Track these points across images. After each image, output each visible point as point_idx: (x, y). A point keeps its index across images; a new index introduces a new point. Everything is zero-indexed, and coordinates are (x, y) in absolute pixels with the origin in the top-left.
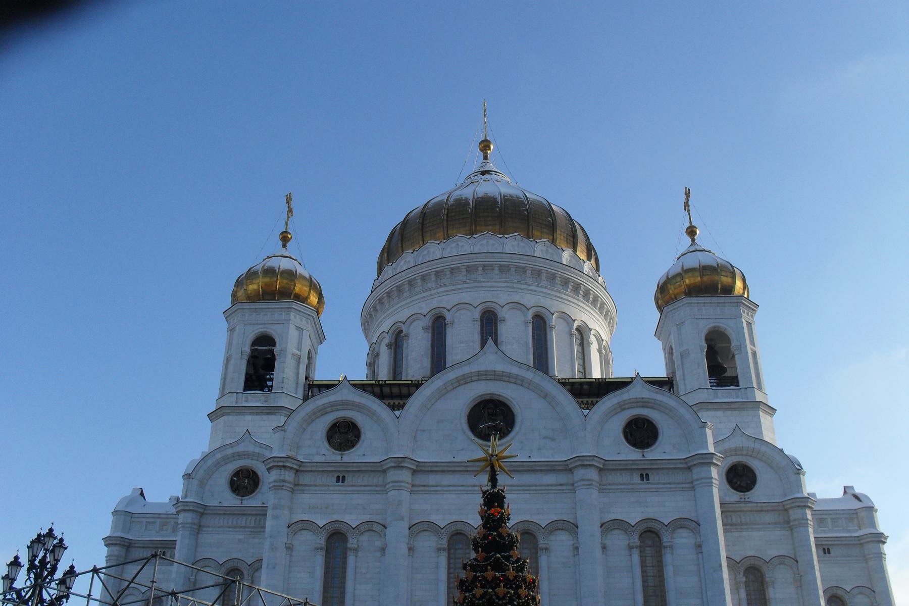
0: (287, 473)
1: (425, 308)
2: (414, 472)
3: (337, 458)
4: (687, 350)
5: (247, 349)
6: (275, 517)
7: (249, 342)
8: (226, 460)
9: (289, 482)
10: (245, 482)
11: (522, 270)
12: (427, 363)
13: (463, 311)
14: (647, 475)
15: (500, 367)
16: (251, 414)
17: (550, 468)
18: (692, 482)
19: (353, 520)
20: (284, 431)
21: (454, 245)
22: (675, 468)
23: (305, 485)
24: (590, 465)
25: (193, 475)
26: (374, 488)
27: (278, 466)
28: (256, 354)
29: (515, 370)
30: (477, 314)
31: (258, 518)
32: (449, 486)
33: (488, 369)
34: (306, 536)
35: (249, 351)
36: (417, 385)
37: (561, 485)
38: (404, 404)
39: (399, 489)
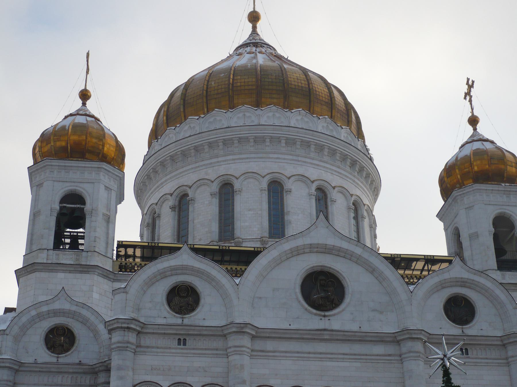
0: (130, 334)
1: (212, 174)
2: (254, 337)
3: (179, 321)
4: (476, 232)
5: (57, 207)
6: (121, 378)
7: (58, 199)
9: (132, 344)
10: (60, 339)
11: (306, 144)
12: (215, 227)
13: (251, 180)
14: (466, 349)
15: (332, 241)
16: (64, 271)
17: (380, 339)
18: (507, 359)
20: (126, 293)
21: (241, 115)
22: (491, 345)
23: (148, 347)
24: (417, 338)
25: (7, 332)
26: (215, 352)
27: (121, 328)
28: (65, 211)
29: (345, 245)
30: (265, 184)
31: (75, 376)
32: (286, 352)
33: (320, 242)
35: (58, 208)
36: (254, 254)
37: (390, 355)
38: (243, 272)
39: (241, 354)
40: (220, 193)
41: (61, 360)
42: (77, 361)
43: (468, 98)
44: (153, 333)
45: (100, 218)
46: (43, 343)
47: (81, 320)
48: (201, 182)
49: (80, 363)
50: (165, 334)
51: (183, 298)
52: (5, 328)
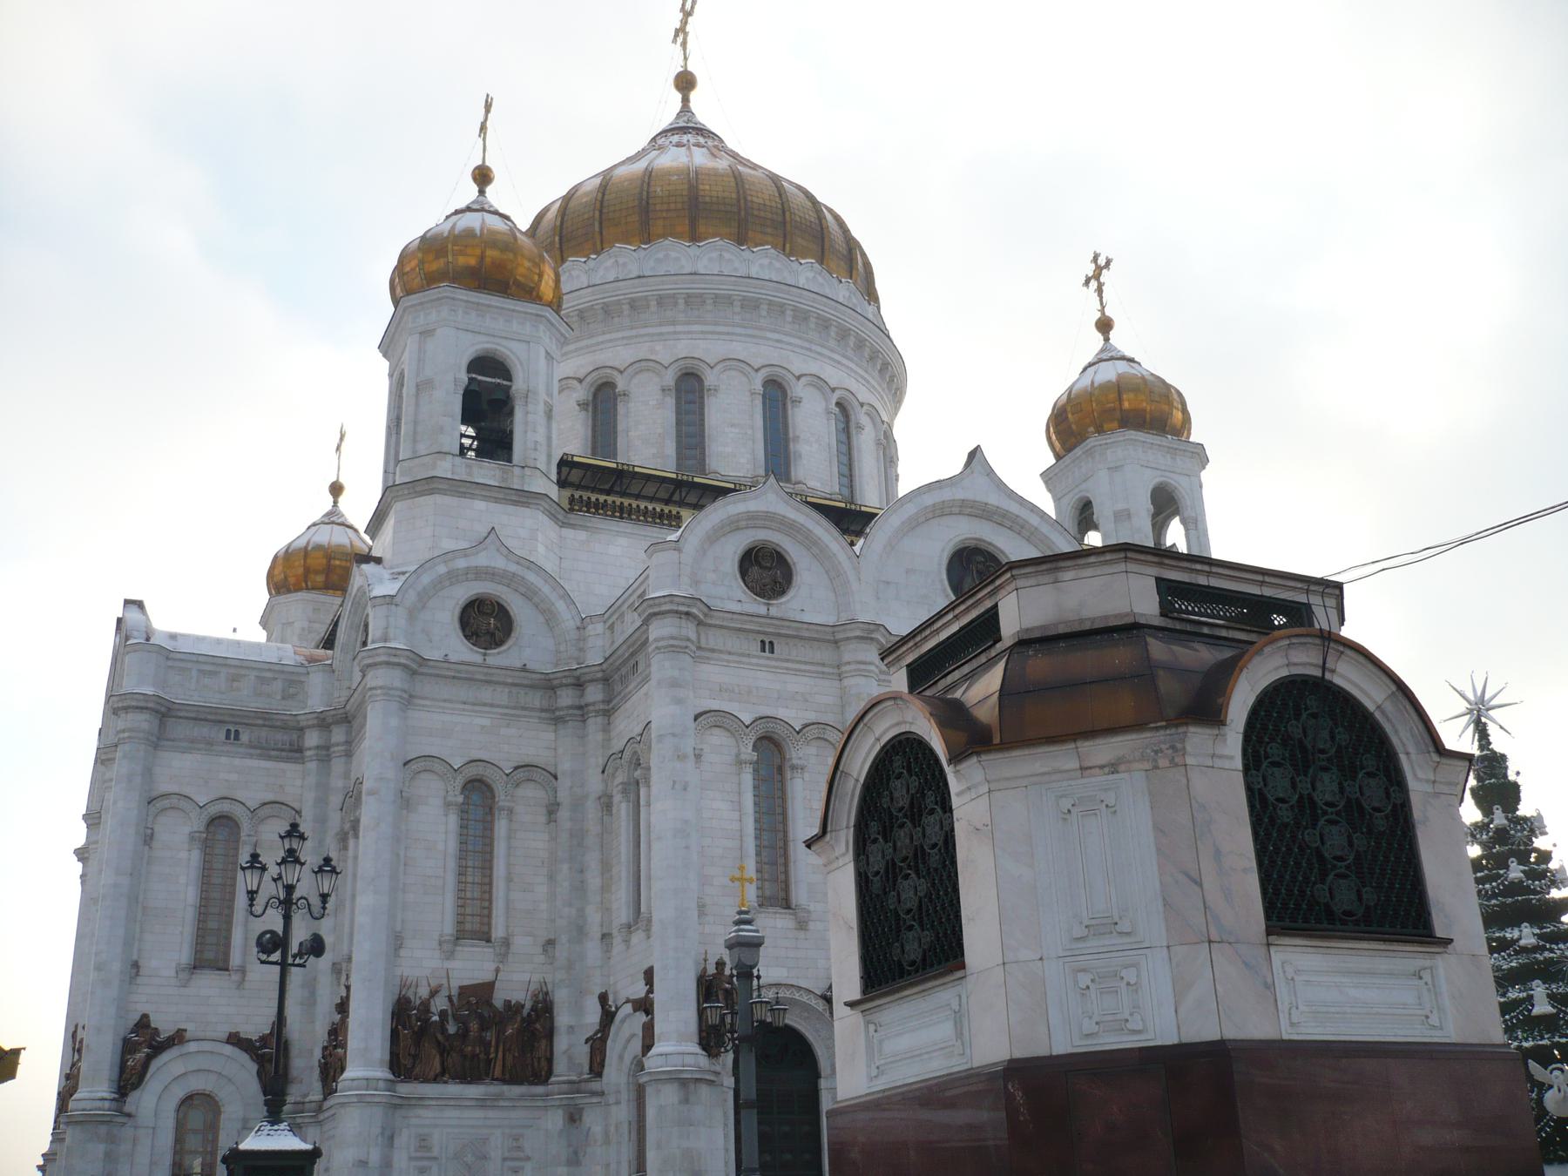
3: (762, 610)
4: (1128, 510)
8: (453, 577)
13: (733, 373)
16: (485, 498)
19: (794, 716)
20: (679, 550)
23: (713, 651)
25: (397, 600)
26: (820, 669)
27: (677, 612)
28: (474, 387)
31: (514, 690)
34: (718, 738)
40: (678, 390)
41: (491, 660)
42: (519, 665)
43: (1094, 284)
44: (721, 627)
45: (541, 408)
46: (457, 625)
47: (523, 590)
48: (643, 365)
49: (524, 669)
50: (739, 630)
51: (766, 570)
52: (393, 593)
